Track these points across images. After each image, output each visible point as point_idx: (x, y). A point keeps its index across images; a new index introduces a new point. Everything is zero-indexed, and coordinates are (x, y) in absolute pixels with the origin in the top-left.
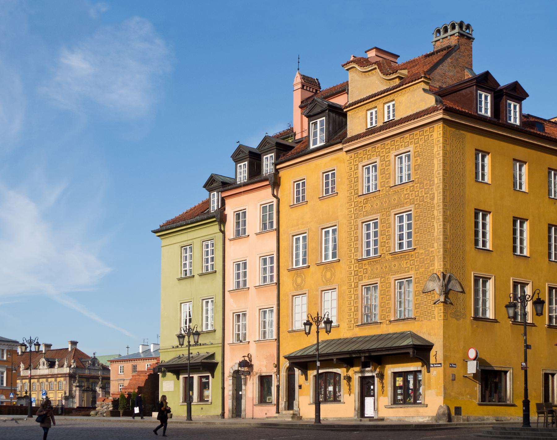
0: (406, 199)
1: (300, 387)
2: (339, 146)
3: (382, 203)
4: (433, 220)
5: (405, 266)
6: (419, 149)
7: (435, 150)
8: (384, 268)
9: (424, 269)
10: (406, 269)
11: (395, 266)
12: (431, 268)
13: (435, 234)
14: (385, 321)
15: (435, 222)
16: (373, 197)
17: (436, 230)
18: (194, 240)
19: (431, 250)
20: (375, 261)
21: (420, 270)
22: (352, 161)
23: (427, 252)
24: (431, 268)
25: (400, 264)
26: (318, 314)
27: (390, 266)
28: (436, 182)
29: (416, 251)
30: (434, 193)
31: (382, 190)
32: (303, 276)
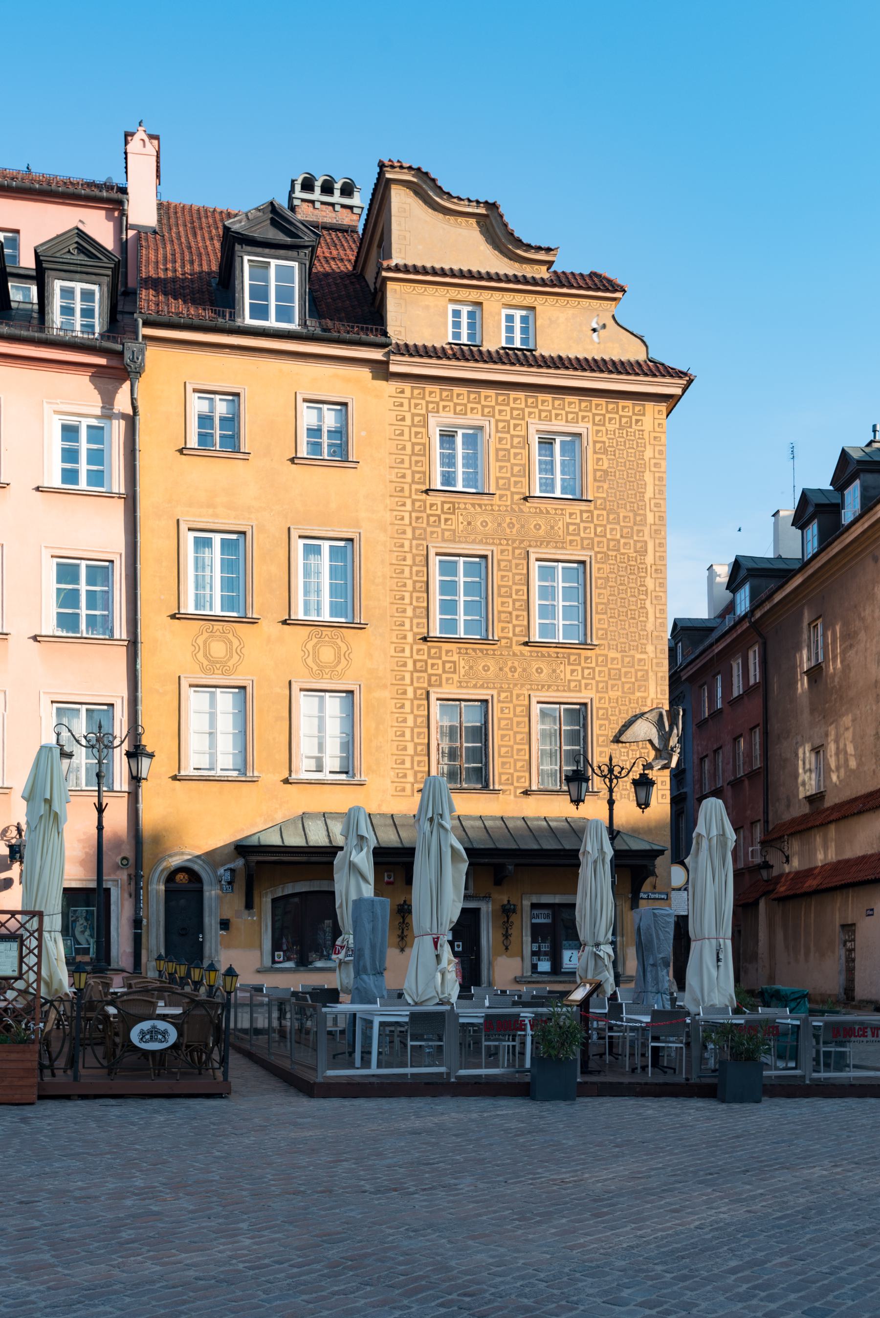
0: (569, 534)
1: (225, 925)
3: (499, 525)
4: (642, 597)
5: (568, 677)
8: (507, 669)
9: (620, 693)
10: (573, 684)
11: (539, 671)
12: (638, 694)
13: (650, 626)
14: (511, 788)
15: (648, 602)
16: (473, 505)
20: (481, 650)
21: (610, 693)
22: (406, 402)
23: (627, 660)
24: (638, 694)
25: (554, 671)
26: (611, 759)
27: (524, 670)
29: (597, 651)
30: (646, 542)
31: (501, 496)
32: (236, 643)
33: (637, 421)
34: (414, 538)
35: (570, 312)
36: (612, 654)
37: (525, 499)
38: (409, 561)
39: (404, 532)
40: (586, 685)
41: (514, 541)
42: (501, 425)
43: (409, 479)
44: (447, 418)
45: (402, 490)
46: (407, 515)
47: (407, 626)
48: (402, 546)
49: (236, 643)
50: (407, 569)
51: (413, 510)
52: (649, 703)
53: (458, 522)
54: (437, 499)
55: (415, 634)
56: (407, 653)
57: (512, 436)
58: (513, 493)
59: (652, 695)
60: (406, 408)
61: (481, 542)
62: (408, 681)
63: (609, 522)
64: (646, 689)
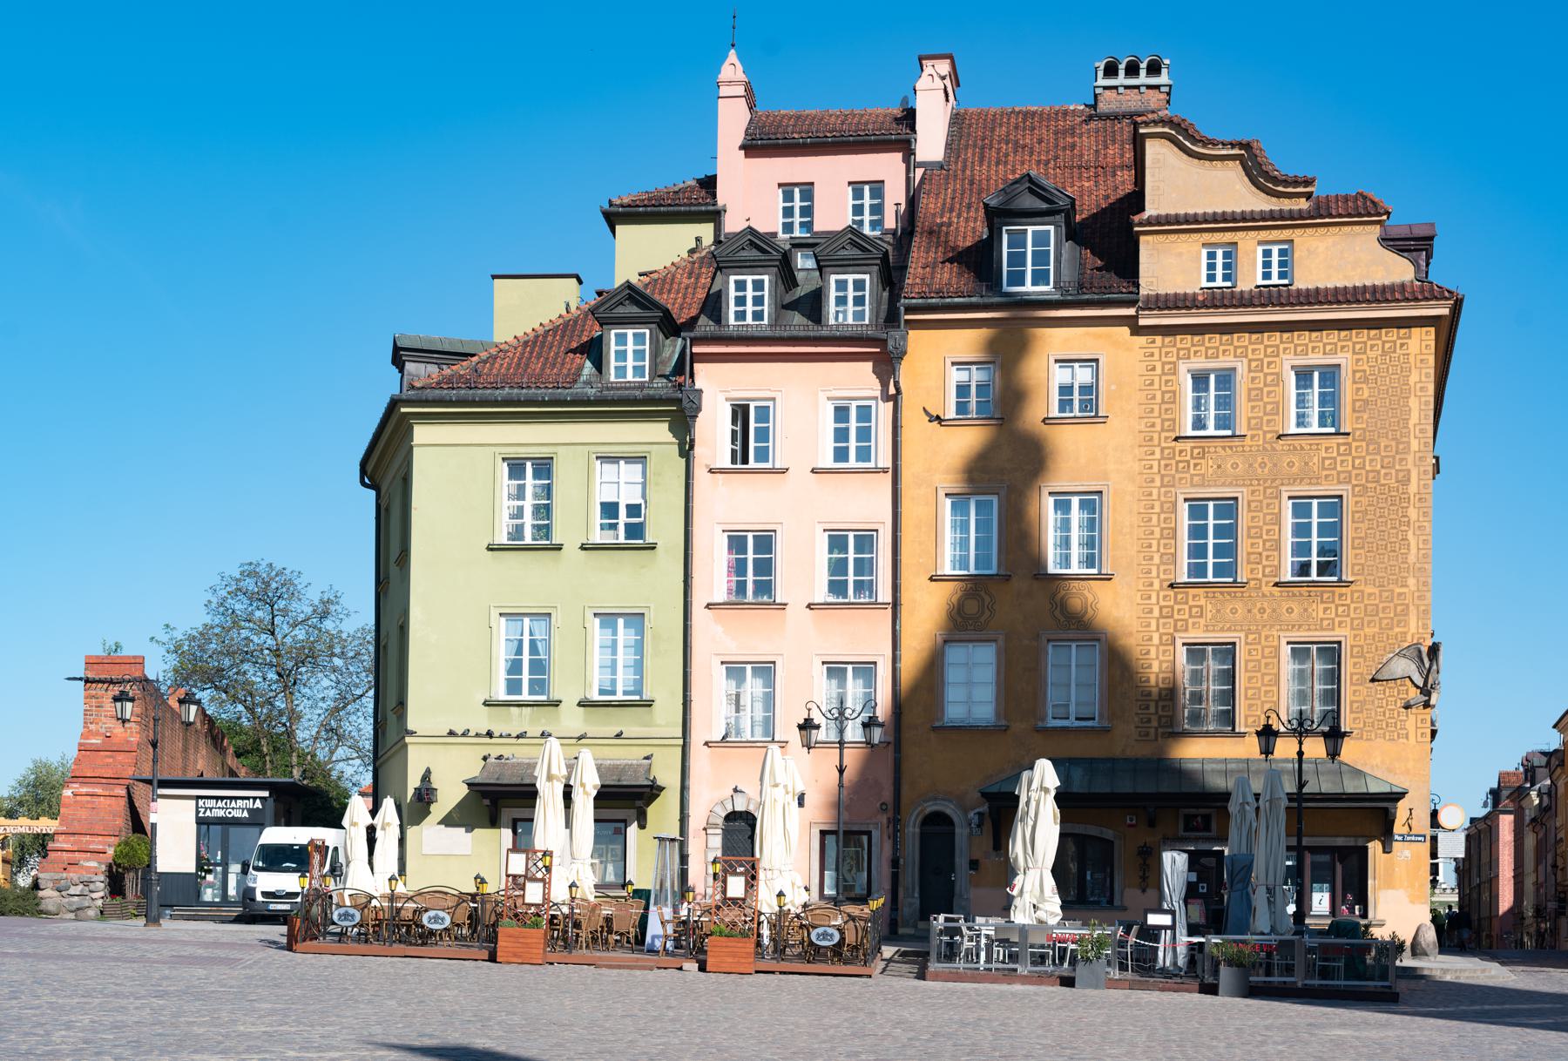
2: (1131, 311)
5: (1321, 615)
6: (1366, 367)
7: (1414, 378)
11: (1290, 611)
12: (1397, 630)
13: (1412, 558)
15: (1410, 534)
16: (1224, 448)
17: (1413, 550)
18: (560, 449)
19: (1398, 590)
22: (1156, 352)
24: (1397, 630)
28: (1414, 445)
29: (1353, 587)
31: (1253, 437)
32: (987, 599)
33: (1402, 345)
34: (1162, 486)
35: (1330, 240)
36: (1369, 589)
37: (1279, 437)
38: (1157, 510)
39: (1153, 481)
40: (1340, 623)
41: (1265, 481)
42: (1254, 364)
43: (1158, 428)
44: (1200, 363)
45: (1151, 439)
46: (1155, 464)
47: (1154, 573)
48: (1150, 494)
49: (987, 599)
50: (1155, 517)
51: (1163, 458)
52: (1409, 638)
53: (1207, 466)
54: (1188, 445)
55: (1162, 581)
56: (1154, 600)
57: (1266, 375)
58: (1265, 433)
59: (1413, 629)
60: (1156, 357)
61: (1231, 484)
62: (1153, 627)
63: (1368, 453)
64: (1407, 624)
